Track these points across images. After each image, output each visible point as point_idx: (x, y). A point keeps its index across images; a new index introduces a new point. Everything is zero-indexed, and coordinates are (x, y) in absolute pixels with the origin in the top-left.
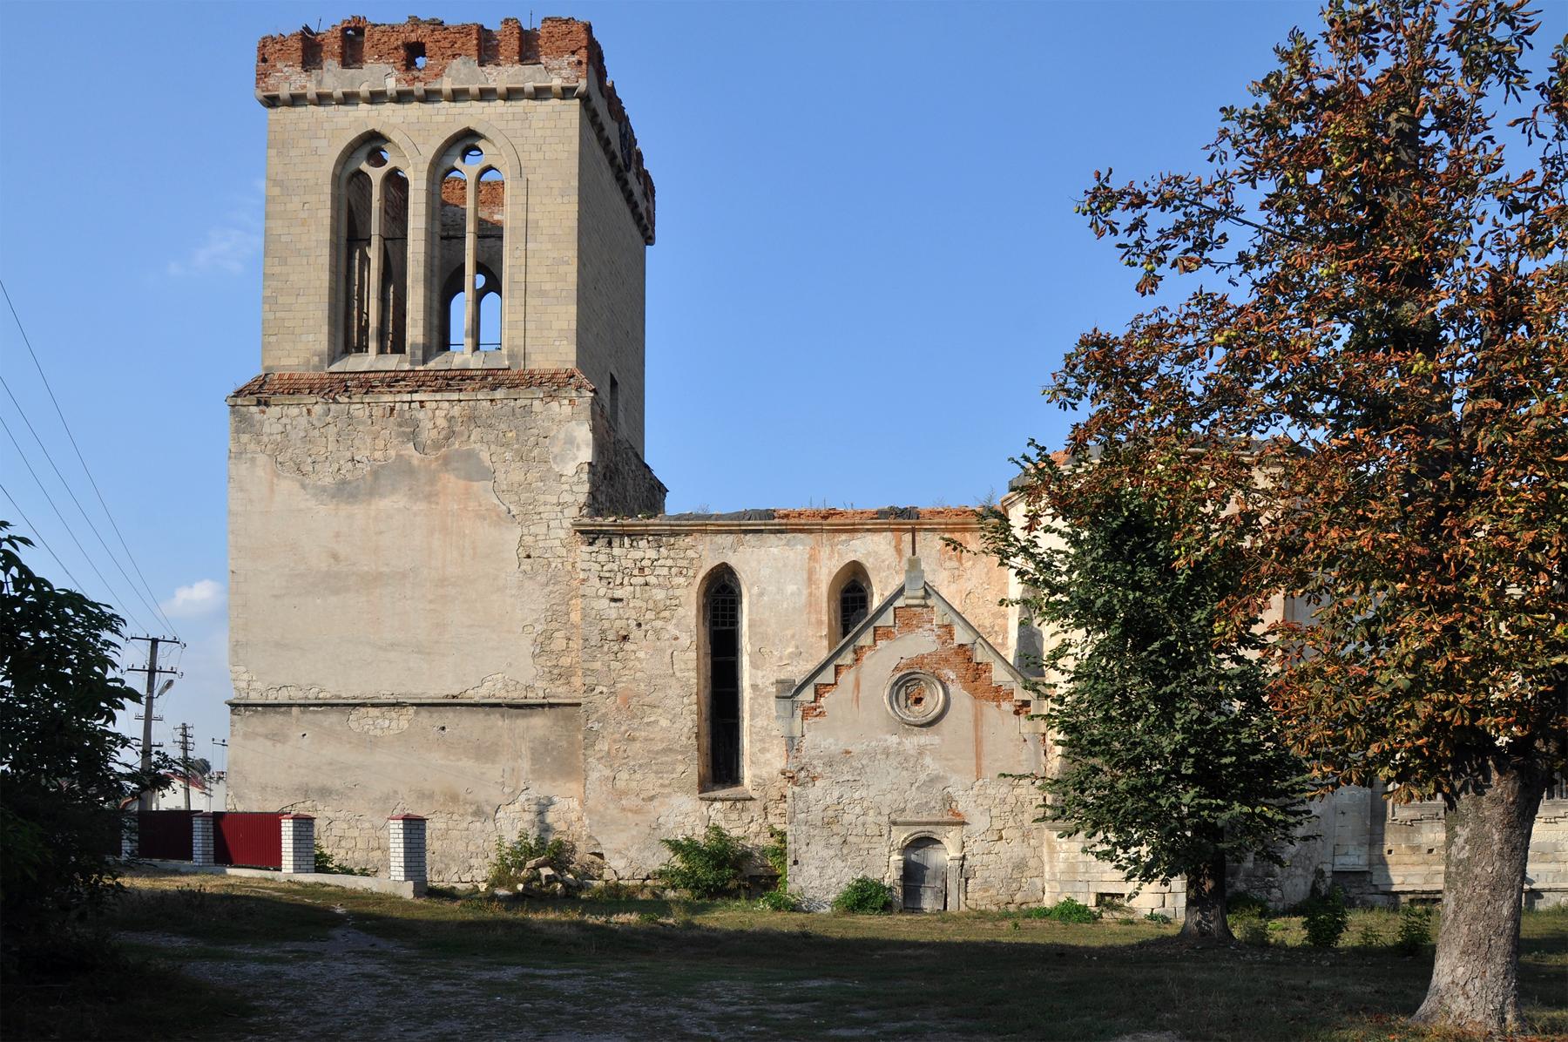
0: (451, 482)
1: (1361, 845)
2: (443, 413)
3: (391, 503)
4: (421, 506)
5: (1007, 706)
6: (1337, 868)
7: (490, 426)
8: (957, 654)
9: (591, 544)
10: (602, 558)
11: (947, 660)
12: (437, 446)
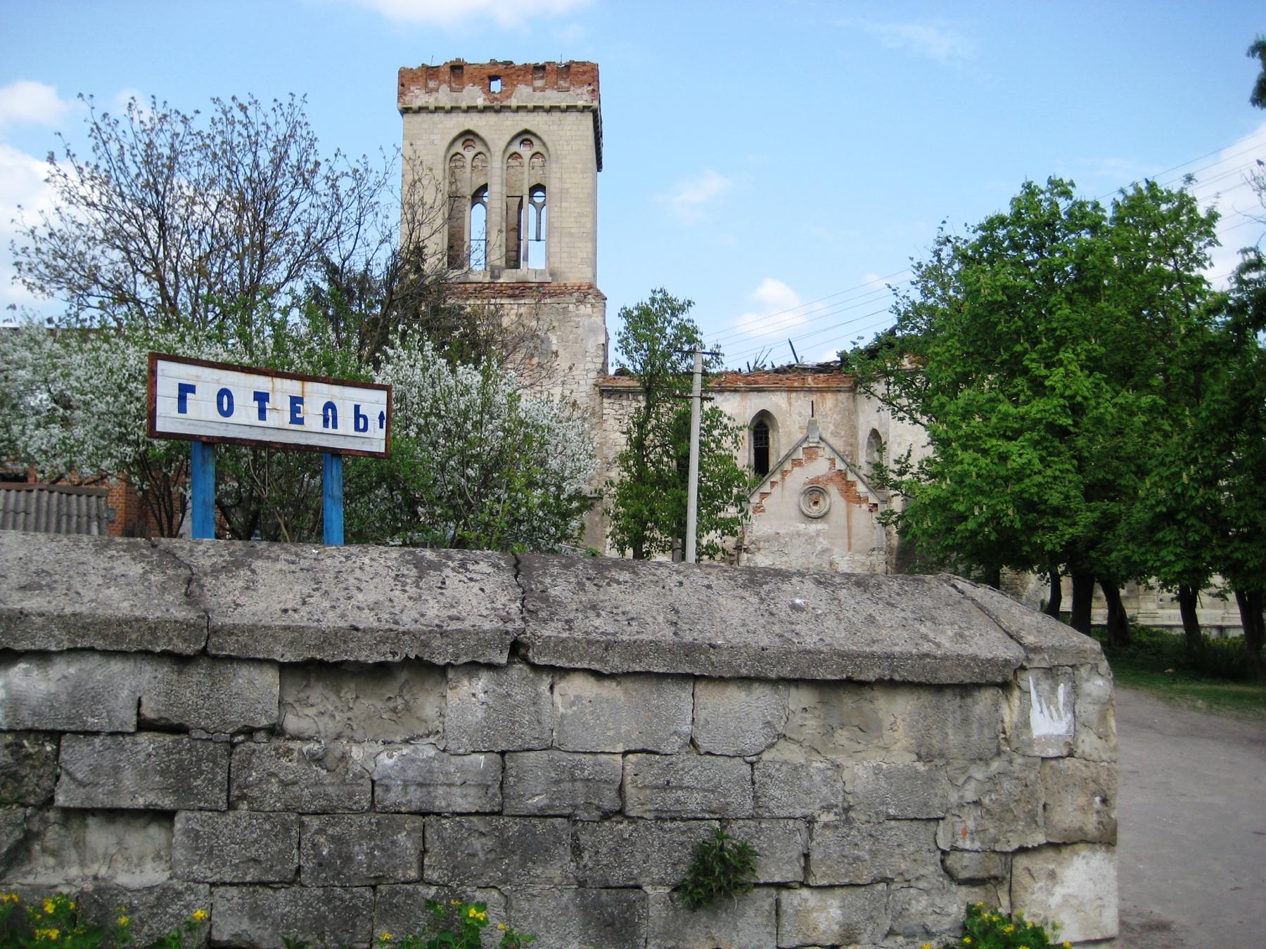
5: (865, 507)
10: (616, 407)
11: (831, 479)
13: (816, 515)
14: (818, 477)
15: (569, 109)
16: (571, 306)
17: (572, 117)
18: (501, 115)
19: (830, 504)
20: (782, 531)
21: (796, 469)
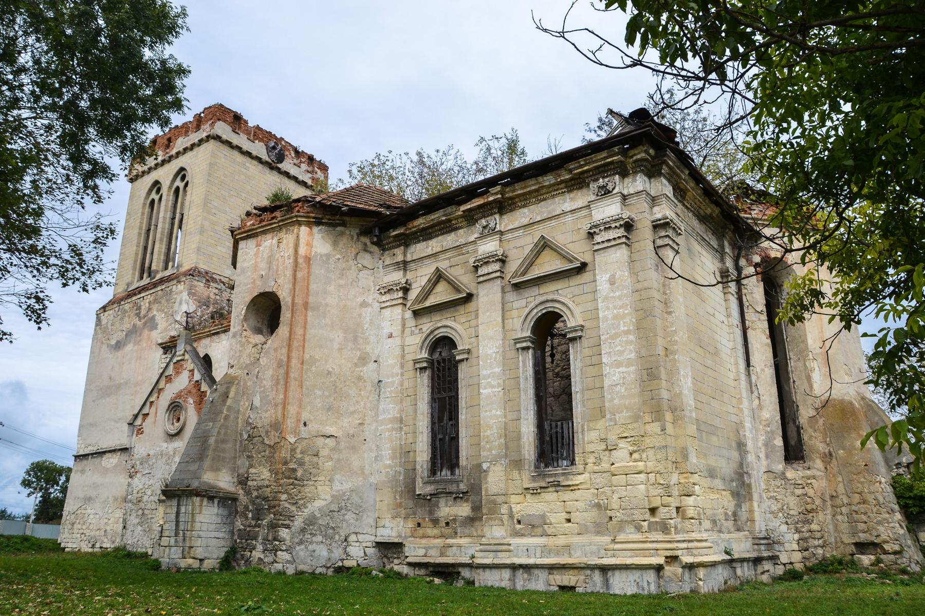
2: (148, 300)
3: (129, 347)
4: (136, 347)
6: (379, 539)
7: (160, 302)
9: (166, 354)
12: (145, 316)
13: (176, 431)
15: (201, 142)
16: (174, 286)
17: (204, 146)
19: (186, 418)
20: (152, 453)
21: (168, 385)
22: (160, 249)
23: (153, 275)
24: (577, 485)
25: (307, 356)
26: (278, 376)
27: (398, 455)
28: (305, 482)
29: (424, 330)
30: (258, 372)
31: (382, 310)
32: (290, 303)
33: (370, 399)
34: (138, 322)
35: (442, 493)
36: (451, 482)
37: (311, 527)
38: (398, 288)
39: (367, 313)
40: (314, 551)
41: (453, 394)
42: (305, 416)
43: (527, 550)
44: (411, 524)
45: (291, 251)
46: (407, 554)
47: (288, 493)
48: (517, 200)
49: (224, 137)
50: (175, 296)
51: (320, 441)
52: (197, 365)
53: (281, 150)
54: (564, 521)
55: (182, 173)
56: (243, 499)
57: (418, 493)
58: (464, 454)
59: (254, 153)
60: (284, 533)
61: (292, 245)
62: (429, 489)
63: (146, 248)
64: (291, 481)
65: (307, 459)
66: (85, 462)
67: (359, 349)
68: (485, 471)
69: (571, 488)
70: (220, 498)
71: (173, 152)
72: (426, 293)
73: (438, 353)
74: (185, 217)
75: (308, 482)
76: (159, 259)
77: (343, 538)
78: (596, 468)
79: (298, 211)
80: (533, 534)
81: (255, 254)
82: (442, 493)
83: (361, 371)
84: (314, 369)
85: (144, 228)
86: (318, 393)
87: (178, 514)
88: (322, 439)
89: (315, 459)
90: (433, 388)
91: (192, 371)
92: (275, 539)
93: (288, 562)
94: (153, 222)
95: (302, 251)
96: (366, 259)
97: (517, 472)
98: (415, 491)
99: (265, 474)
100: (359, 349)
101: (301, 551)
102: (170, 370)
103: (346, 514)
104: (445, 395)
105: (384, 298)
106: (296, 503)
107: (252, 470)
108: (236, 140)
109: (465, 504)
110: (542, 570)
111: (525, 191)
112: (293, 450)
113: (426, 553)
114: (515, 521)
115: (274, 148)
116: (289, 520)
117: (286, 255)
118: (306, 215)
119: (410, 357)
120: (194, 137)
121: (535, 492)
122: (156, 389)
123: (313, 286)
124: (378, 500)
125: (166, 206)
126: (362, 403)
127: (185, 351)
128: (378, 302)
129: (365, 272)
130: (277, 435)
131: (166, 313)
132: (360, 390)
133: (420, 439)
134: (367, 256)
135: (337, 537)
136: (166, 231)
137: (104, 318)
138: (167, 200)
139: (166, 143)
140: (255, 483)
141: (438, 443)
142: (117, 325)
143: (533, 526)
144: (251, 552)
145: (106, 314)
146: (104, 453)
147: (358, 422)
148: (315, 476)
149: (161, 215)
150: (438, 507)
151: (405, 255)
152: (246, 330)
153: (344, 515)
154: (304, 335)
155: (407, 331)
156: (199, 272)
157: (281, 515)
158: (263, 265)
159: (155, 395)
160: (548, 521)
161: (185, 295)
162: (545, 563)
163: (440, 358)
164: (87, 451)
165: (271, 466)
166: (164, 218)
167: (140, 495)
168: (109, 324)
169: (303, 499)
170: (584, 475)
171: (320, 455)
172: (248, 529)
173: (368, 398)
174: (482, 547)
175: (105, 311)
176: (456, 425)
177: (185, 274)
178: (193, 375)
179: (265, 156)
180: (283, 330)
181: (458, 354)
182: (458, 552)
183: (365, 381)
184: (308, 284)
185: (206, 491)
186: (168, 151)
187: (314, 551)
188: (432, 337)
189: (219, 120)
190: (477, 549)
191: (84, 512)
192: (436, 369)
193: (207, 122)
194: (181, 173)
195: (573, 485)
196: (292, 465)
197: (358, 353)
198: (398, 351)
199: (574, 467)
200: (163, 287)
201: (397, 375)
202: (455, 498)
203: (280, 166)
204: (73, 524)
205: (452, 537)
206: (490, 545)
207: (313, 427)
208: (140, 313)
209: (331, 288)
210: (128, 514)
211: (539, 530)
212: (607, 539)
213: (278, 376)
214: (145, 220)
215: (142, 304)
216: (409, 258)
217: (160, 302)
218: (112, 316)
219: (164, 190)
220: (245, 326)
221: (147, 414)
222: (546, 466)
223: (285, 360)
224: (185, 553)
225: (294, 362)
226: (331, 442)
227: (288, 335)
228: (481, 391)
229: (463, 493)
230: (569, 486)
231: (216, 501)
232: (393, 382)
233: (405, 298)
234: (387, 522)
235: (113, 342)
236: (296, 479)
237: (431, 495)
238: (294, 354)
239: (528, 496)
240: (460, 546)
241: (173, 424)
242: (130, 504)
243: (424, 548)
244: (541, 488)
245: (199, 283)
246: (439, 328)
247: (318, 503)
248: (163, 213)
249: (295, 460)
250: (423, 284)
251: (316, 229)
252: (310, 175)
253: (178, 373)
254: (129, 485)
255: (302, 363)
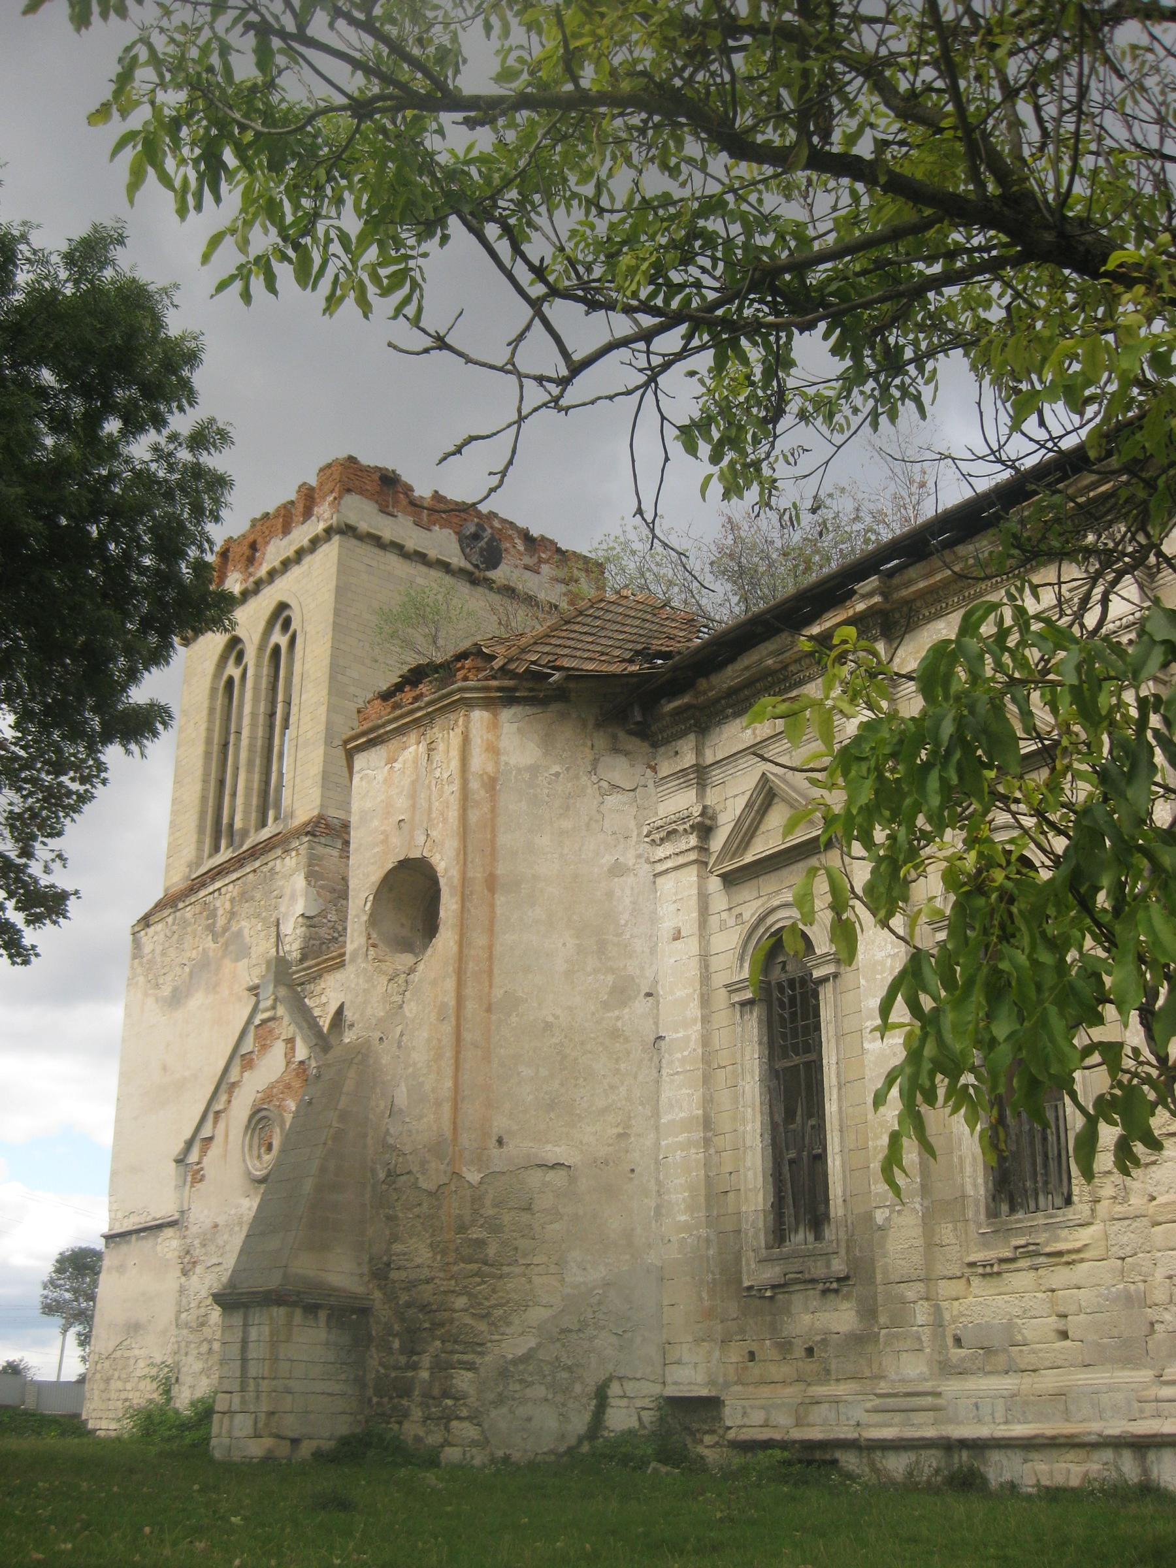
0: (228, 965)
1: (698, 1341)
3: (198, 1000)
6: (671, 1391)
7: (252, 898)
8: (297, 1075)
12: (226, 929)
14: (272, 1087)
15: (315, 543)
16: (278, 862)
18: (261, 596)
20: (221, 1220)
21: (246, 1074)
22: (244, 782)
23: (237, 839)
24: (1078, 1251)
25: (498, 993)
26: (439, 1041)
27: (702, 1200)
28: (506, 1269)
29: (746, 916)
30: (402, 1035)
31: (659, 880)
32: (456, 881)
33: (640, 1078)
34: (213, 946)
35: (796, 1281)
36: (811, 1255)
37: (521, 1367)
38: (687, 826)
39: (626, 889)
40: (529, 1419)
41: (812, 1057)
42: (500, 1123)
43: (977, 1406)
44: (735, 1355)
45: (455, 764)
46: (728, 1423)
47: (470, 1295)
48: (918, 604)
49: (363, 527)
50: (281, 883)
51: (535, 1179)
52: (301, 1028)
53: (492, 539)
54: (1053, 1336)
55: (285, 614)
56: (382, 1311)
57: (746, 1284)
58: (839, 1192)
59: (433, 554)
60: (463, 1381)
61: (455, 753)
62: (771, 1274)
63: (221, 783)
64: (474, 1267)
65: (507, 1218)
66: (124, 1248)
67: (612, 970)
68: (880, 1228)
69: (1064, 1259)
70: (331, 1308)
71: (263, 571)
72: (746, 832)
73: (779, 967)
74: (294, 710)
75: (511, 1269)
76: (247, 804)
77: (591, 1389)
78: (1118, 1208)
79: (465, 679)
80: (988, 1368)
81: (385, 780)
82: (796, 1281)
83: (618, 1018)
84: (514, 1019)
85: (216, 741)
86: (526, 1072)
87: (245, 1343)
88: (539, 1173)
89: (525, 1217)
90: (771, 1044)
91: (290, 1041)
92: (446, 1394)
93: (474, 1443)
94: (233, 728)
95: (479, 761)
96: (619, 770)
97: (950, 1226)
98: (740, 1281)
99: (423, 1255)
100: (612, 970)
101: (499, 1418)
102: (249, 1045)
103: (595, 1337)
104: (797, 1060)
105: (661, 852)
106: (488, 1315)
107: (398, 1247)
108: (388, 529)
109: (846, 1305)
110: (1009, 1452)
111: (932, 581)
112: (477, 1200)
113: (767, 1420)
114: (950, 1341)
115: (476, 537)
116: (475, 1352)
117: (445, 776)
118: (480, 684)
119: (720, 979)
120: (301, 535)
121: (990, 1272)
122: (224, 1085)
123: (505, 839)
124: (665, 1303)
125: (256, 688)
126: (623, 1090)
127: (275, 1000)
128: (648, 861)
129: (613, 800)
130: (442, 1167)
131: (264, 920)
132: (617, 1060)
133: (749, 1164)
134: (621, 762)
135: (578, 1388)
136: (259, 743)
137: (147, 937)
138: (257, 677)
139: (248, 552)
140: (403, 1275)
141: (786, 1169)
142: (172, 953)
143: (988, 1350)
144: (400, 1423)
145: (151, 930)
146: (160, 1227)
147: (616, 1131)
148: (525, 1256)
149: (247, 709)
150: (789, 1313)
151: (699, 752)
152: (374, 946)
153: (592, 1339)
154: (490, 947)
155: (714, 921)
156: (327, 826)
157: (456, 1342)
158: (402, 803)
159: (223, 1098)
160: (1019, 1337)
161: (299, 882)
162: (1013, 1434)
163: (784, 977)
164: (127, 1226)
165: (433, 1235)
166: (254, 715)
167: (203, 1311)
168: (158, 951)
169: (502, 1305)
170: (1092, 1228)
171: (535, 1207)
172: (393, 1375)
173: (635, 1078)
174: (878, 1401)
175: (148, 926)
176: (820, 1128)
177: (298, 833)
178: (293, 1049)
179: (457, 559)
180: (446, 939)
181: (817, 966)
182: (833, 1415)
183: (627, 1040)
184: (494, 836)
185: (298, 1293)
186: (251, 570)
187: (529, 1419)
188: (761, 930)
189: (349, 491)
190: (869, 1405)
191: (127, 1354)
192: (776, 1003)
193: (324, 498)
194: (281, 615)
195: (1069, 1252)
196: (476, 1233)
197: (610, 979)
198: (693, 970)
199: (1071, 1209)
200: (257, 864)
201: (694, 1021)
202: (825, 1292)
203: (491, 574)
204: (107, 1381)
205: (821, 1382)
206: (895, 1395)
207: (518, 1148)
208: (214, 924)
209: (544, 841)
210: (183, 1351)
211: (1001, 1359)
212: (1145, 1375)
213: (439, 1041)
214: (218, 723)
215: (218, 904)
216: (709, 758)
217: (252, 898)
218: (162, 936)
219: (250, 657)
220: (374, 936)
221: (211, 1139)
222: (1013, 1210)
223: (452, 1003)
224: (261, 1425)
225: (471, 1006)
226: (557, 1178)
227: (455, 948)
228: (866, 1045)
229: (839, 1280)
230: (1060, 1254)
231: (323, 1315)
232: (688, 1038)
233: (703, 849)
234: (685, 1352)
235: (166, 991)
236: (485, 1263)
237: (773, 1287)
238: (469, 991)
239: (976, 1281)
240: (836, 1401)
241: (259, 1157)
242: (185, 1332)
243: (762, 1408)
244: (1002, 1261)
245: (328, 850)
246: (774, 910)
247: (537, 1315)
248: (249, 704)
249: (482, 1221)
250: (738, 813)
251: (506, 714)
252: (562, 588)
253: (264, 1047)
254: (182, 1290)
255: (489, 1010)
